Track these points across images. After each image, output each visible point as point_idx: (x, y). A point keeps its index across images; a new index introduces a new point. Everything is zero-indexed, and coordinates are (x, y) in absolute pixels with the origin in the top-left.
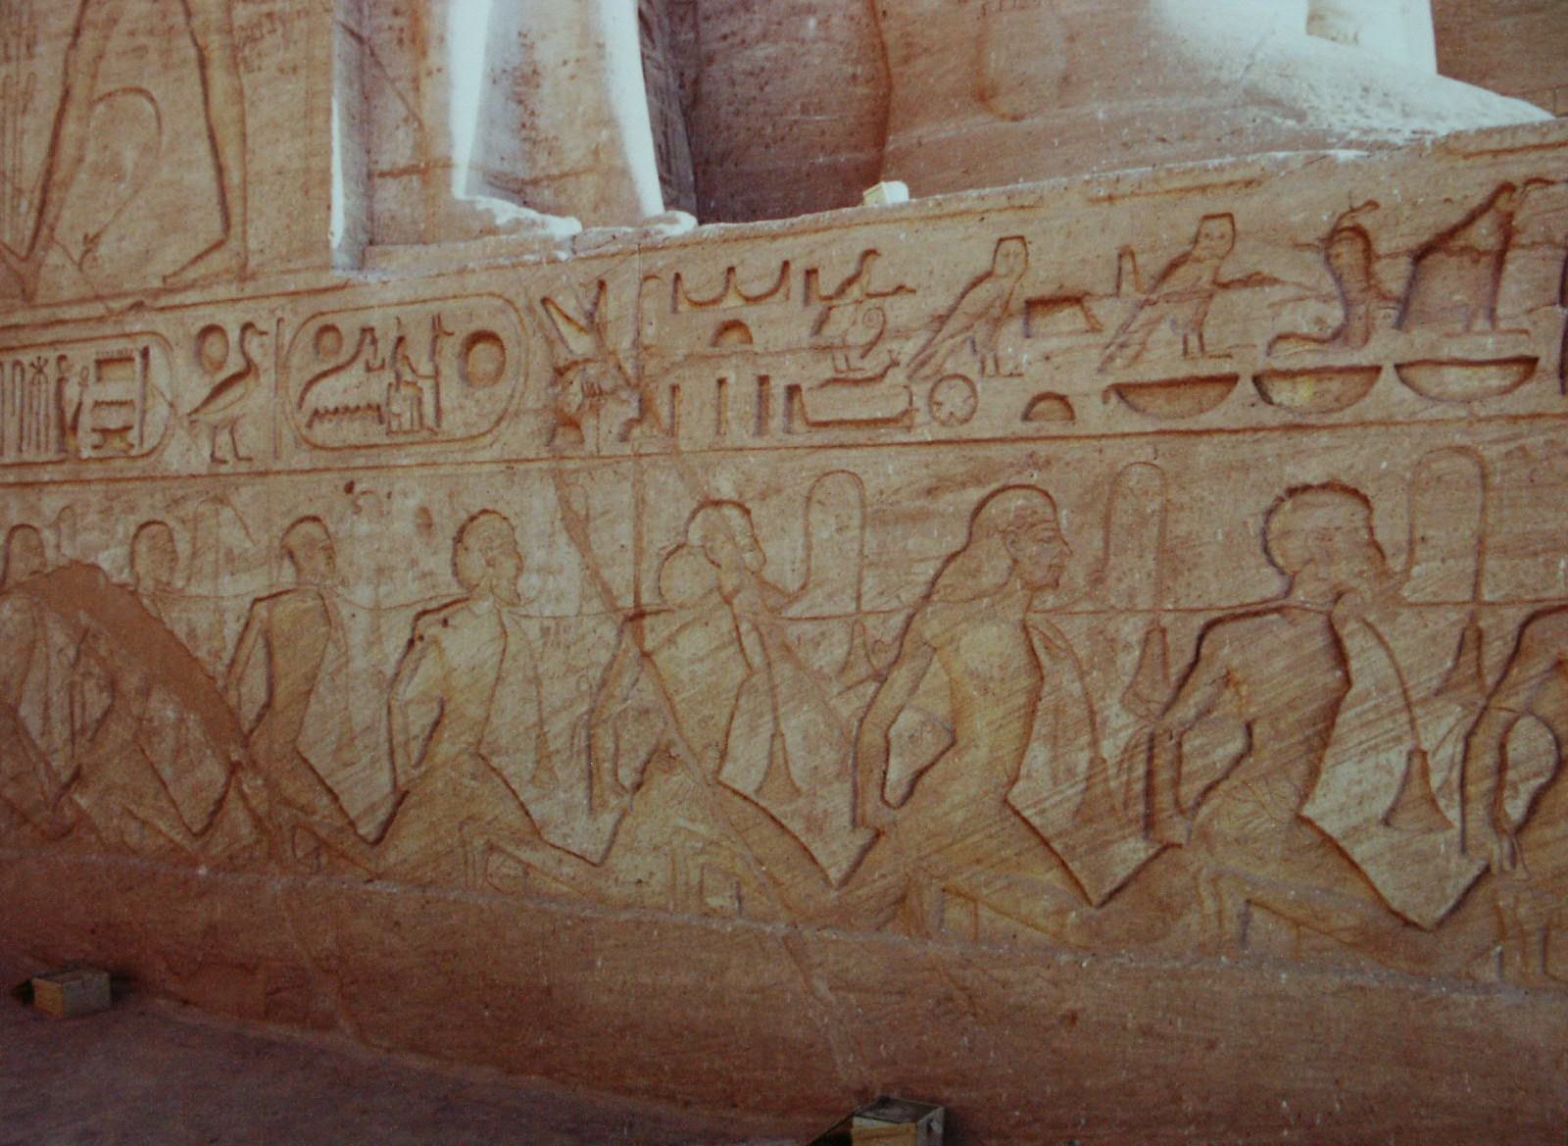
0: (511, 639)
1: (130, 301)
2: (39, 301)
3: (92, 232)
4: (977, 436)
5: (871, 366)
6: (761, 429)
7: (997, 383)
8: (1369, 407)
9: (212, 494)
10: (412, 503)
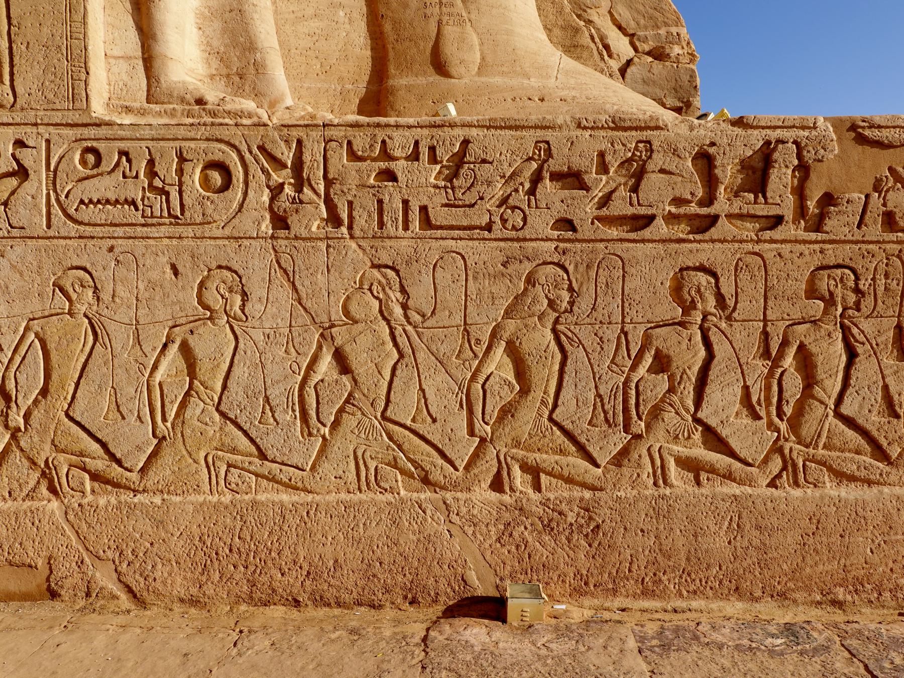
0: (241, 340)
4: (528, 237)
5: (470, 198)
6: (406, 228)
7: (538, 212)
8: (714, 233)
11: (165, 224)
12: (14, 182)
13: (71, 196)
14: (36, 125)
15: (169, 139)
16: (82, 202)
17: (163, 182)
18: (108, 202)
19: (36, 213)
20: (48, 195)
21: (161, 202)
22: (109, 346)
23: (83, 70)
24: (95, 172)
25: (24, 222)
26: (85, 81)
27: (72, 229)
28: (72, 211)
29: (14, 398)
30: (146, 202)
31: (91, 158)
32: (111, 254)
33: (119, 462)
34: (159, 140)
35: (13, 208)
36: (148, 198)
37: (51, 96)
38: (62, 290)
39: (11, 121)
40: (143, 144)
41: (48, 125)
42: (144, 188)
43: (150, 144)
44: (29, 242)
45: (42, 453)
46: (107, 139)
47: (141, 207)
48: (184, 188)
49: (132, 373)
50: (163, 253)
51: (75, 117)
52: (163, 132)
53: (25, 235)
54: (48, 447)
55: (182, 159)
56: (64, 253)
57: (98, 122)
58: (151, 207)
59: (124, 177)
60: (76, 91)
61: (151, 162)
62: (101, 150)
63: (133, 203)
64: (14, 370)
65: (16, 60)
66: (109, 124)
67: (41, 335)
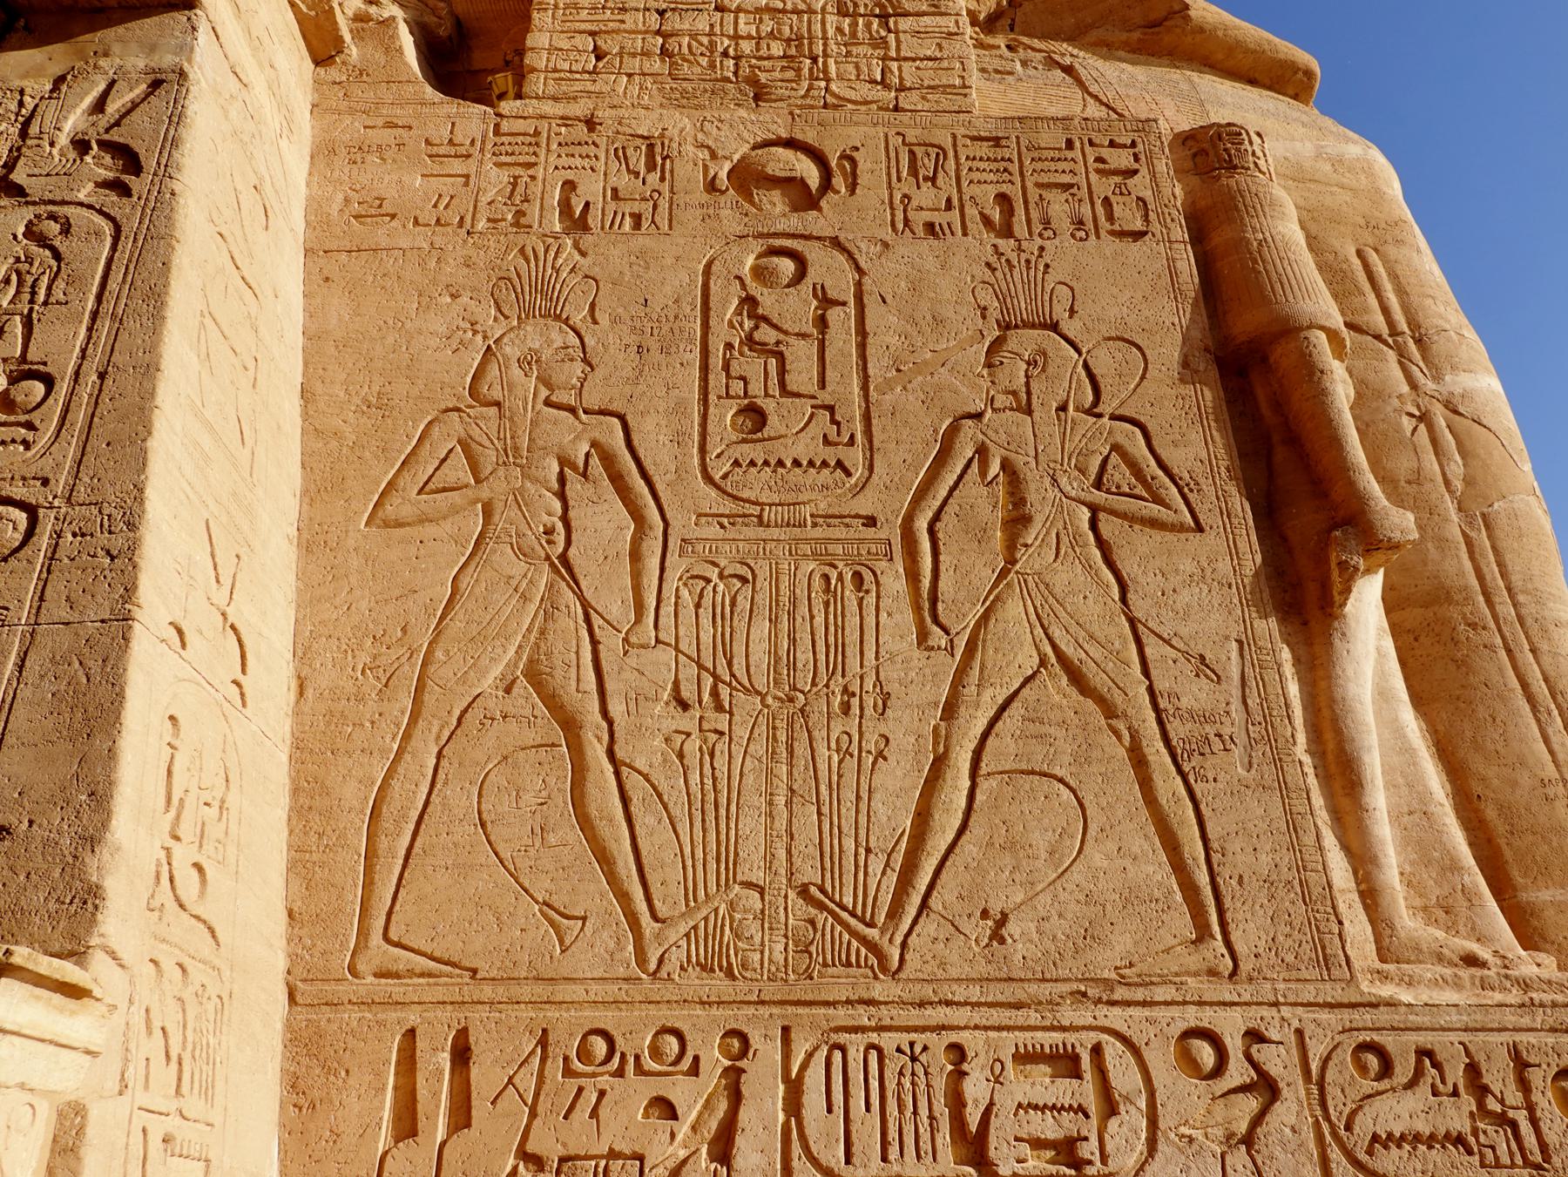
1: (1065, 988)
3: (995, 909)
12: (1251, 1104)
13: (1357, 1129)
14: (1276, 1004)
15: (1492, 1030)
16: (1375, 1138)
17: (1502, 1102)
18: (1417, 1138)
19: (1303, 1159)
20: (1317, 1123)
23: (1333, 918)
24: (1385, 1084)
26: (1340, 935)
30: (1482, 1138)
31: (1373, 1061)
34: (1477, 1030)
35: (1264, 1150)
36: (1485, 1132)
37: (1290, 958)
39: (1237, 999)
40: (1454, 1037)
41: (1295, 1004)
42: (1471, 1113)
43: (1465, 1037)
46: (1393, 1029)
48: (1539, 1114)
52: (1479, 1018)
55: (1521, 1066)
57: (1373, 1000)
58: (1493, 1148)
60: (1328, 951)
61: (1473, 1070)
62: (1389, 1048)
63: (1459, 1140)
65: (1228, 903)
66: (1391, 1004)
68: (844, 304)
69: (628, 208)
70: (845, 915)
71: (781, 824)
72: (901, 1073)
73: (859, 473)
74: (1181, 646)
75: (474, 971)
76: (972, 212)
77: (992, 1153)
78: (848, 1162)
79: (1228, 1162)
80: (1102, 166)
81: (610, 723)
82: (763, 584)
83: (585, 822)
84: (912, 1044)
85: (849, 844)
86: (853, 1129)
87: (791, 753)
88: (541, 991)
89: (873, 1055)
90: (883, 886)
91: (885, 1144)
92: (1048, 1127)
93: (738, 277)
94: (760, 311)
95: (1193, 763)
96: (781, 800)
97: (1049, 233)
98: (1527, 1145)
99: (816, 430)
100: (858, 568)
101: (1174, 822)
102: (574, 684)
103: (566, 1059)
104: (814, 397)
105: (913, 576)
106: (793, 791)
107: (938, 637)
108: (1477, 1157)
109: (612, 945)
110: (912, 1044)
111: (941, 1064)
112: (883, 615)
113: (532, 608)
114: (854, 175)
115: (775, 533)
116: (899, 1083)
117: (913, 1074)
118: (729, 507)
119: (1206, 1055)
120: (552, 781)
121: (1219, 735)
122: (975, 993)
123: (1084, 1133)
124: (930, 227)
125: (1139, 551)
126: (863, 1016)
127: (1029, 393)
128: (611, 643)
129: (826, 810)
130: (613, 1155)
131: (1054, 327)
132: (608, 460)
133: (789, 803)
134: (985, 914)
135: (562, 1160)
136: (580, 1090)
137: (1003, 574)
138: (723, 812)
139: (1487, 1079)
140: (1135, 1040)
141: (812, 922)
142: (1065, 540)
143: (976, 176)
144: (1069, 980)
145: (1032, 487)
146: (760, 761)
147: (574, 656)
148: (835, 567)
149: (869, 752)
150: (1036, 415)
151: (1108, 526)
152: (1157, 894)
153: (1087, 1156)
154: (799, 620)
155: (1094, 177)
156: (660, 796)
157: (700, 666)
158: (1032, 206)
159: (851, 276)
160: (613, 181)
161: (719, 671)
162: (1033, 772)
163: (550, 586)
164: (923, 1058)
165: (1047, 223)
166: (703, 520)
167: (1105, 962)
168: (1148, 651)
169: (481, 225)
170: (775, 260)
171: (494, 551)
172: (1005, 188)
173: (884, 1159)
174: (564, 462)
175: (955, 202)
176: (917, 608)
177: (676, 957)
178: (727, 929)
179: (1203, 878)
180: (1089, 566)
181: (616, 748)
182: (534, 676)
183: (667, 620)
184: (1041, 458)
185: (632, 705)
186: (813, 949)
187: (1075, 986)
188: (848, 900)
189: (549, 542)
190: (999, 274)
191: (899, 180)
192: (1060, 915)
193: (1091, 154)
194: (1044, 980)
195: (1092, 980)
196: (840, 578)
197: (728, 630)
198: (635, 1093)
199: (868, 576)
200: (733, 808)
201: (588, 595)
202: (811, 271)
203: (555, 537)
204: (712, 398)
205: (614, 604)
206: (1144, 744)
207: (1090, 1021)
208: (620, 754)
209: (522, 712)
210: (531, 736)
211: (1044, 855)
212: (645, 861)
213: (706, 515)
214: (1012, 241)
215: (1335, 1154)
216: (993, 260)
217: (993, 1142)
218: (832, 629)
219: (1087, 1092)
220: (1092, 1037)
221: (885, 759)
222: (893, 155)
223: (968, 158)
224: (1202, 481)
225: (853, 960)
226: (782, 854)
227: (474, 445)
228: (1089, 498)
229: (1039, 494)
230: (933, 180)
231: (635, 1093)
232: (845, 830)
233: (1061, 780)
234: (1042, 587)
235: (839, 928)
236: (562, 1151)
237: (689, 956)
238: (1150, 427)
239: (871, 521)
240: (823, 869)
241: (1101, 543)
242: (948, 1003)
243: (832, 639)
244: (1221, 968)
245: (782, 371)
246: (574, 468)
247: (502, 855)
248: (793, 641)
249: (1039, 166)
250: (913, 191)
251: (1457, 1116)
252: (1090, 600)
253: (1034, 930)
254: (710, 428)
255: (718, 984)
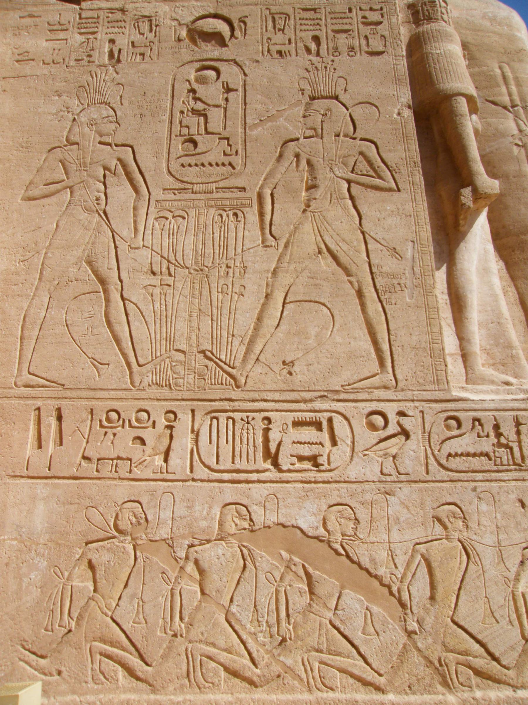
2: (248, 388)
3: (288, 360)
9: (383, 490)
10: (513, 497)
11: (511, 470)
16: (450, 455)
17: (507, 439)
21: (507, 454)
22: (480, 565)
23: (443, 363)
25: (410, 470)
27: (444, 475)
28: (444, 462)
29: (409, 605)
31: (453, 423)
32: (474, 493)
33: (494, 658)
35: (400, 460)
37: (421, 381)
38: (439, 520)
39: (395, 398)
40: (490, 413)
42: (493, 445)
44: (413, 485)
45: (436, 653)
47: (493, 459)
48: (523, 444)
49: (500, 585)
50: (513, 492)
51: (440, 395)
53: (410, 479)
54: (439, 647)
56: (440, 493)
58: (501, 458)
59: (479, 436)
61: (497, 427)
64: (406, 584)
65: (396, 357)
67: (427, 556)
68: (236, 90)
69: (138, 50)
70: (222, 364)
71: (195, 324)
72: (242, 429)
73: (238, 168)
74: (385, 244)
75: (64, 385)
76: (300, 45)
77: (280, 461)
78: (217, 463)
79: (384, 465)
80: (364, 20)
81: (121, 281)
82: (192, 221)
83: (109, 323)
84: (248, 417)
85: (225, 334)
86: (220, 450)
87: (201, 293)
88: (91, 394)
89: (231, 421)
90: (239, 351)
91: (233, 456)
92: (306, 451)
93: (188, 81)
94: (197, 95)
95: (386, 297)
96: (195, 315)
97: (337, 54)
98: (515, 456)
99: (220, 149)
100: (235, 211)
101: (374, 322)
102: (106, 266)
103: (100, 421)
104: (220, 134)
105: (261, 214)
106: (200, 310)
107: (271, 241)
108: (493, 462)
109: (120, 376)
110: (248, 417)
111: (260, 425)
112: (246, 233)
113: (89, 234)
114: (245, 30)
115: (198, 196)
116: (241, 433)
117: (248, 429)
118: (179, 185)
119: (379, 420)
120: (96, 307)
121: (399, 284)
122: (277, 396)
123: (321, 453)
124: (280, 53)
125: (368, 201)
126: (226, 405)
127: (322, 129)
128: (123, 246)
129: (215, 318)
130: (119, 458)
131: (336, 98)
132: (124, 166)
133: (199, 316)
134: (284, 363)
135: (99, 460)
136: (106, 433)
137: (304, 211)
138: (169, 320)
139: (502, 430)
140: (348, 415)
141: (207, 366)
142: (334, 196)
143: (304, 27)
144: (320, 391)
145: (321, 172)
146: (186, 297)
147: (106, 253)
148: (226, 211)
149: (236, 293)
150: (324, 139)
151: (356, 190)
152: (364, 354)
153: (322, 462)
154: (207, 235)
155: (361, 26)
156: (142, 313)
157: (162, 257)
158: (329, 40)
159: (241, 77)
160: (132, 38)
161: (170, 258)
162: (311, 301)
163: (98, 223)
164: (252, 422)
165: (336, 49)
166: (166, 191)
167: (336, 384)
168: (369, 246)
169: (73, 63)
170: (206, 72)
171: (73, 209)
172: (317, 33)
173: (233, 463)
174: (105, 168)
175: (293, 41)
176: (262, 229)
177: (147, 380)
178: (169, 369)
179: (385, 347)
180: (345, 208)
181: (123, 292)
182: (90, 263)
183: (148, 237)
184: (326, 159)
185: (131, 275)
186: (206, 378)
187: (322, 393)
188: (223, 357)
189: (98, 204)
190: (311, 73)
191: (266, 31)
192: (318, 363)
193: (360, 14)
194: (309, 391)
195: (331, 391)
196: (228, 215)
197: (175, 240)
198: (126, 435)
199: (240, 214)
200: (174, 318)
201: (114, 226)
202: (222, 76)
203: (100, 202)
204: (173, 136)
205: (125, 231)
206: (364, 287)
207: (329, 408)
208: (125, 296)
209: (84, 278)
210: (88, 289)
211: (313, 337)
212: (134, 340)
213: (168, 189)
214: (319, 58)
215: (432, 461)
216: (310, 68)
217: (281, 456)
218: (222, 238)
219: (325, 436)
220: (329, 414)
221: (243, 295)
222: (264, 19)
223: (300, 19)
224: (402, 168)
225: (224, 383)
226: (194, 337)
227: (67, 163)
228: (346, 176)
229: (324, 176)
230: (283, 30)
231: (126, 435)
232: (223, 327)
233: (324, 305)
234: (321, 217)
235: (218, 369)
236: (99, 456)
237: (152, 380)
238: (378, 143)
239: (243, 189)
240: (212, 344)
241: (352, 198)
242: (265, 401)
243: (222, 243)
244: (390, 386)
245: (206, 123)
246: (110, 170)
247: (75, 338)
248: (204, 244)
249: (334, 21)
250: (272, 36)
251: (486, 445)
252: (344, 224)
253: (306, 370)
254: (171, 150)
255: (166, 393)
